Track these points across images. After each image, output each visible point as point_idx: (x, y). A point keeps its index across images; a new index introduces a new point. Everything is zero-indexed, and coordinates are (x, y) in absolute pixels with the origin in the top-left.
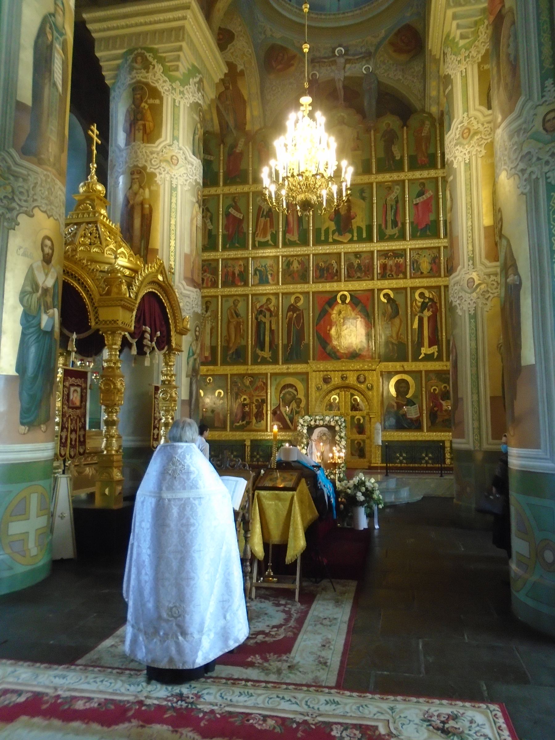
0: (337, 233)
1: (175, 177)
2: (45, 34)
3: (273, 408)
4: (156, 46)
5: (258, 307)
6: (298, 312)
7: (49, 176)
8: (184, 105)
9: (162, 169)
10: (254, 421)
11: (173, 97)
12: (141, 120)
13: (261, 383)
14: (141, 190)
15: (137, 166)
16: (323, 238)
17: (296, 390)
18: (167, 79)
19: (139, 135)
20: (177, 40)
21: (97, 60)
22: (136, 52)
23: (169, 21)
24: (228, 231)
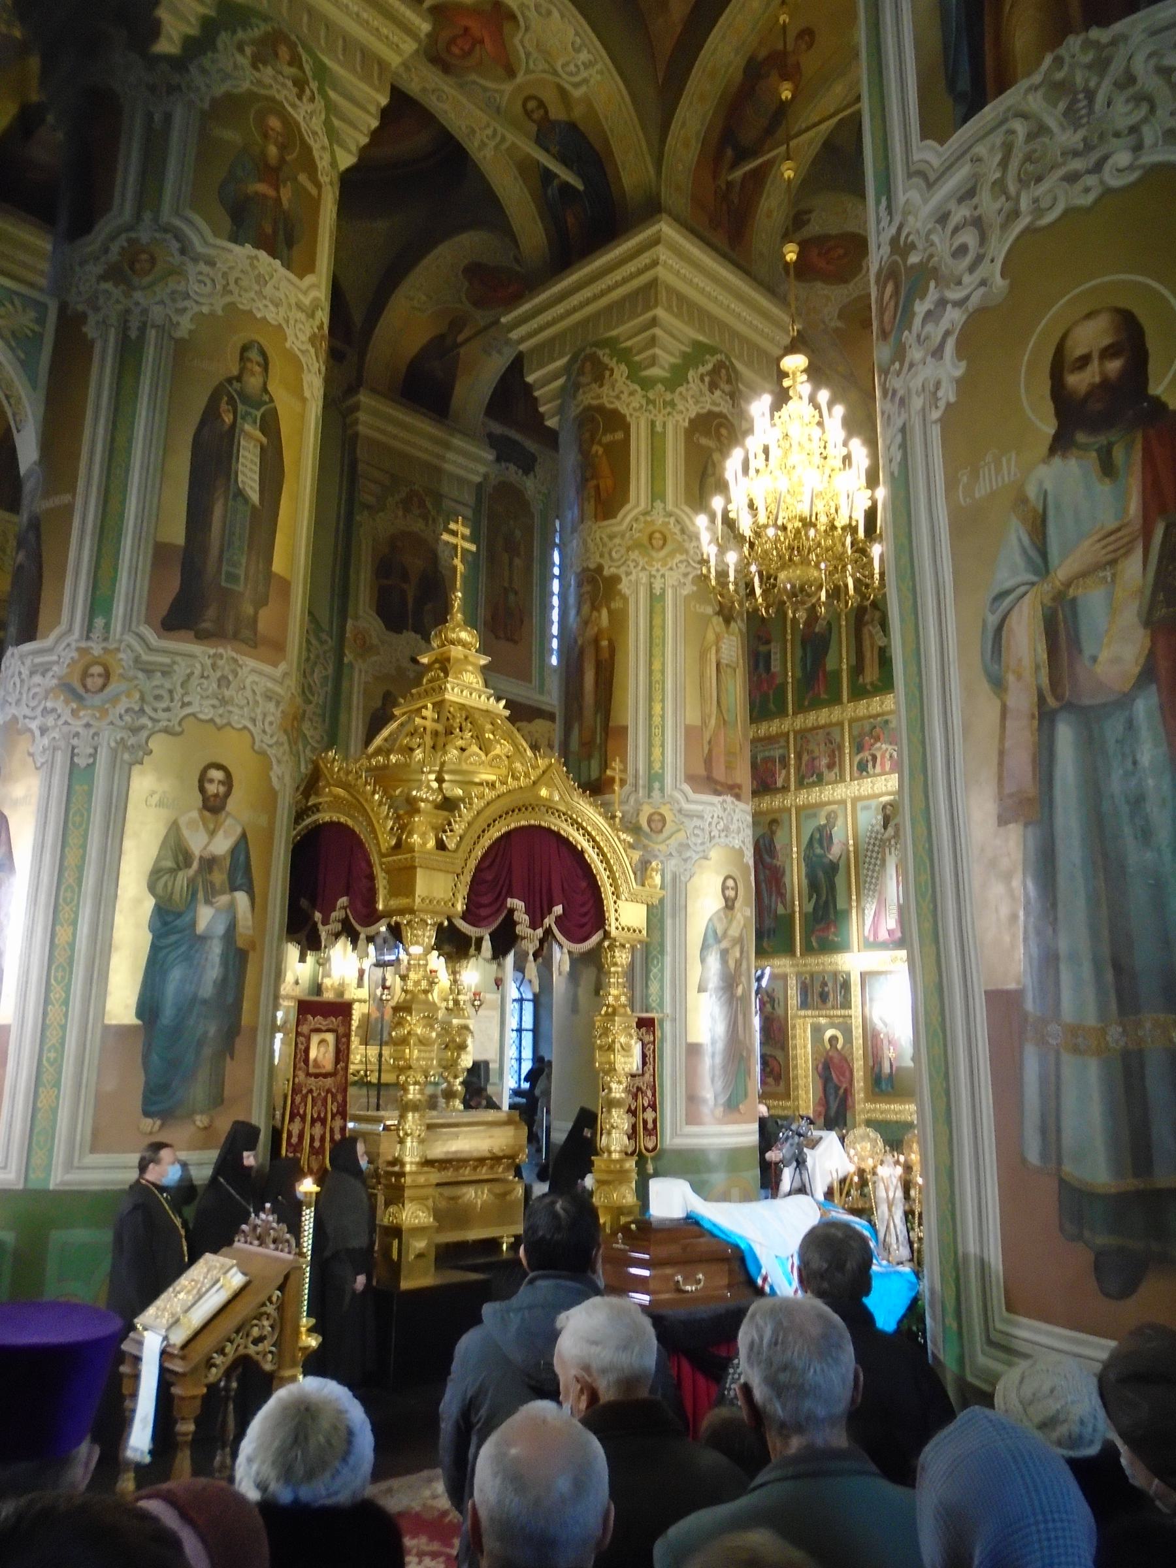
1: (658, 575)
2: (219, 416)
4: (614, 333)
7: (221, 657)
8: (676, 426)
9: (632, 565)
11: (651, 417)
12: (592, 478)
14: (595, 614)
15: (587, 569)
18: (638, 389)
19: (590, 507)
20: (648, 307)
21: (528, 389)
22: (582, 356)
23: (632, 276)
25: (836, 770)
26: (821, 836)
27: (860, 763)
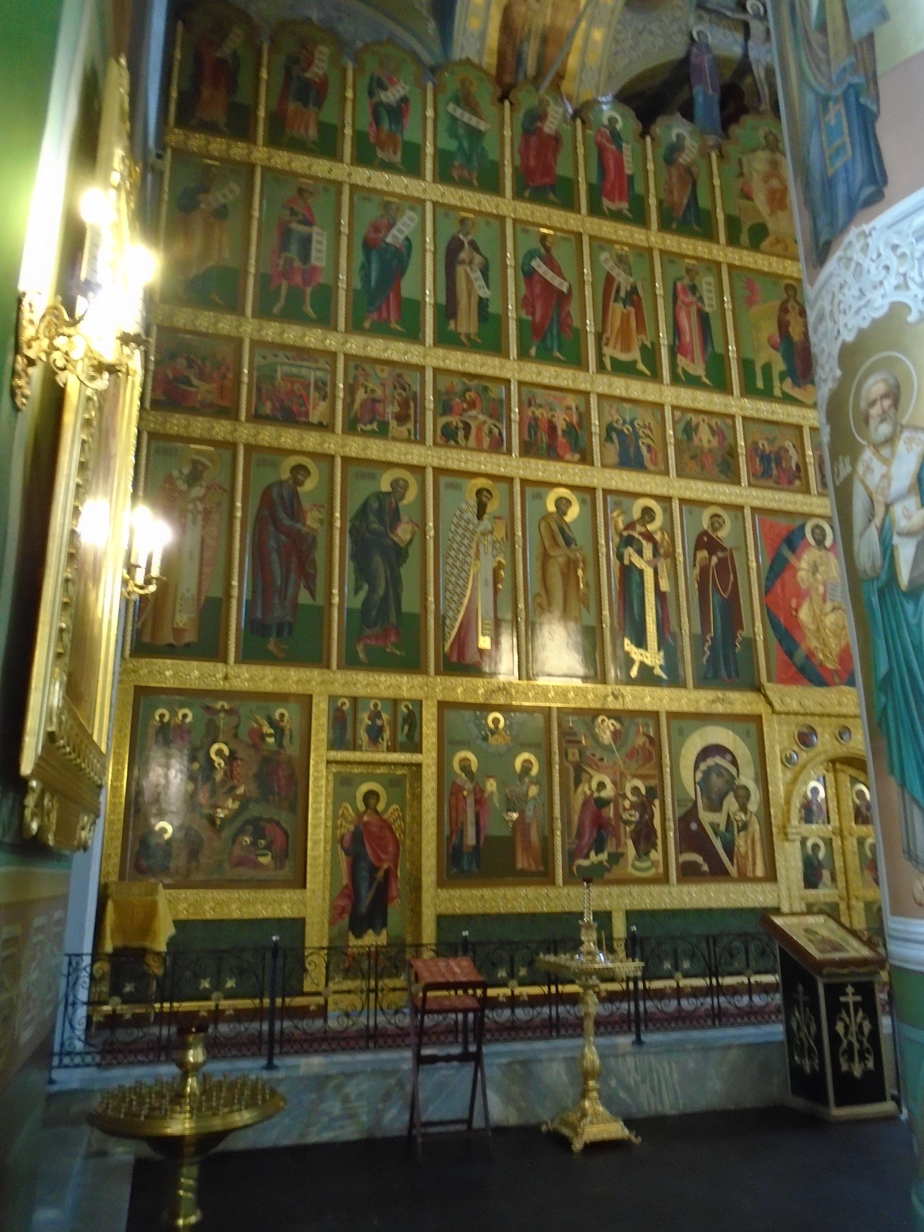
0: (789, 381)
3: (680, 812)
5: (621, 526)
6: (720, 554)
10: (631, 851)
13: (641, 740)
16: (760, 384)
17: (734, 762)
24: (533, 315)
25: (410, 425)
26: (381, 505)
27: (446, 427)
